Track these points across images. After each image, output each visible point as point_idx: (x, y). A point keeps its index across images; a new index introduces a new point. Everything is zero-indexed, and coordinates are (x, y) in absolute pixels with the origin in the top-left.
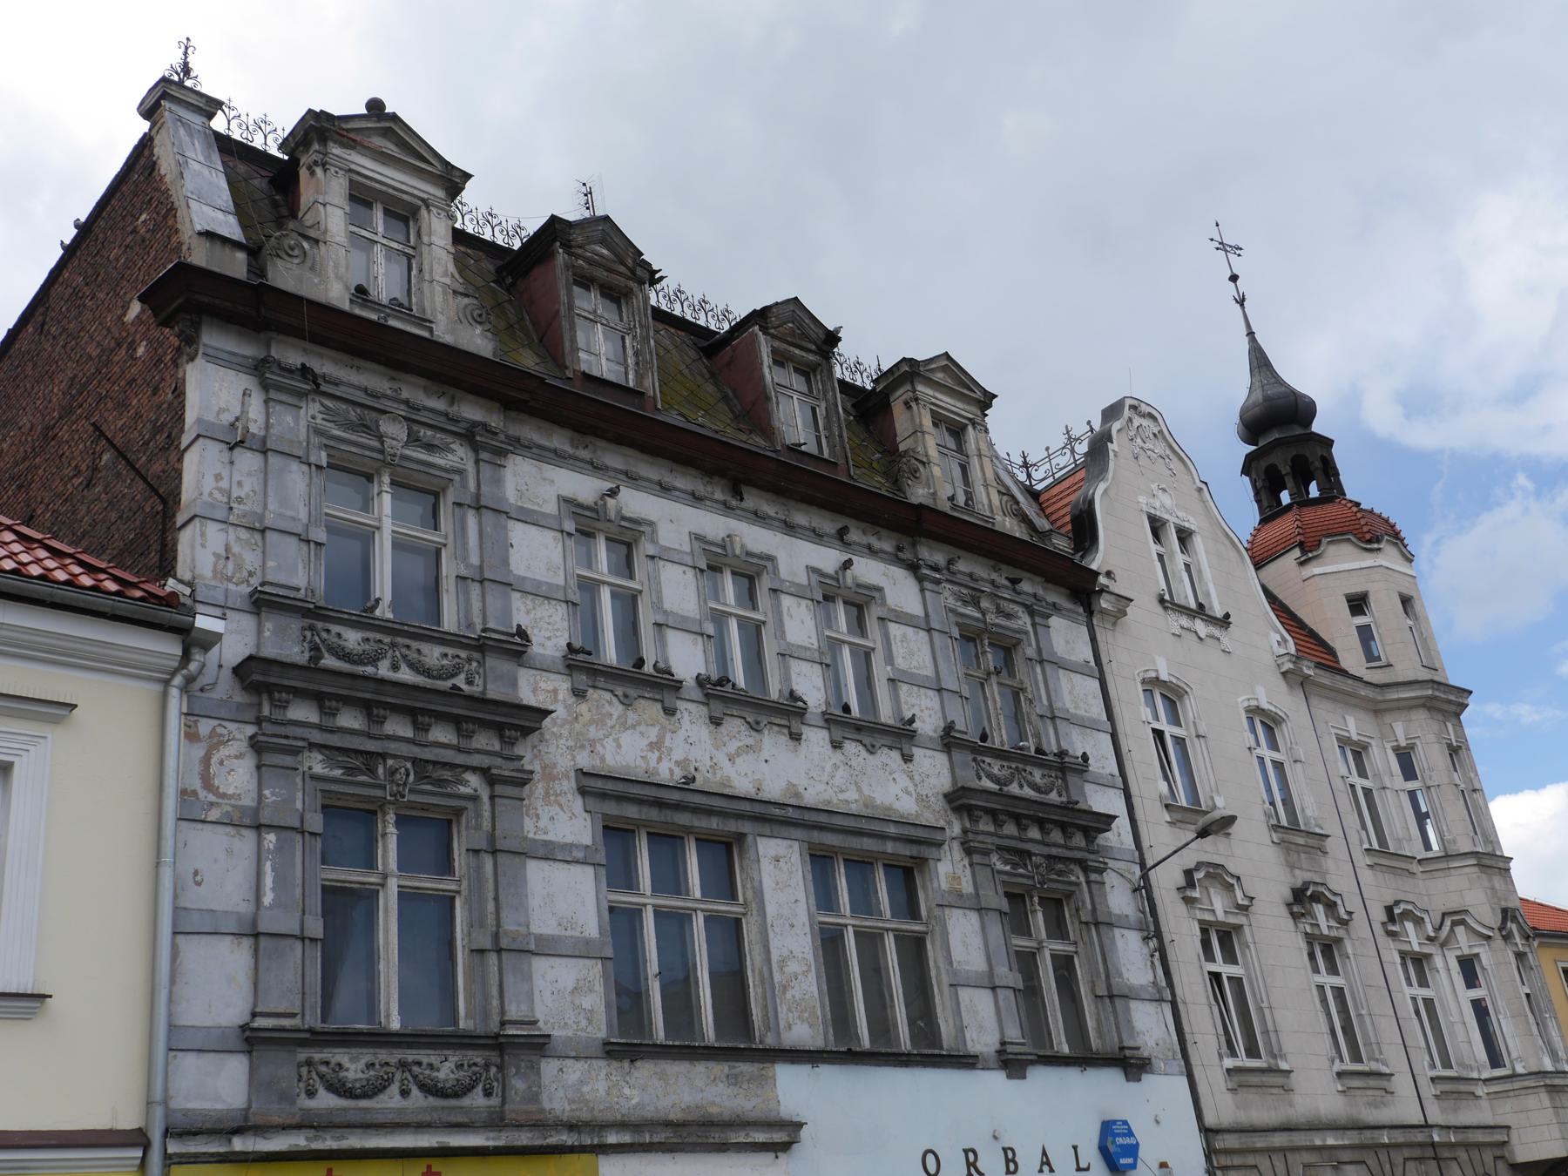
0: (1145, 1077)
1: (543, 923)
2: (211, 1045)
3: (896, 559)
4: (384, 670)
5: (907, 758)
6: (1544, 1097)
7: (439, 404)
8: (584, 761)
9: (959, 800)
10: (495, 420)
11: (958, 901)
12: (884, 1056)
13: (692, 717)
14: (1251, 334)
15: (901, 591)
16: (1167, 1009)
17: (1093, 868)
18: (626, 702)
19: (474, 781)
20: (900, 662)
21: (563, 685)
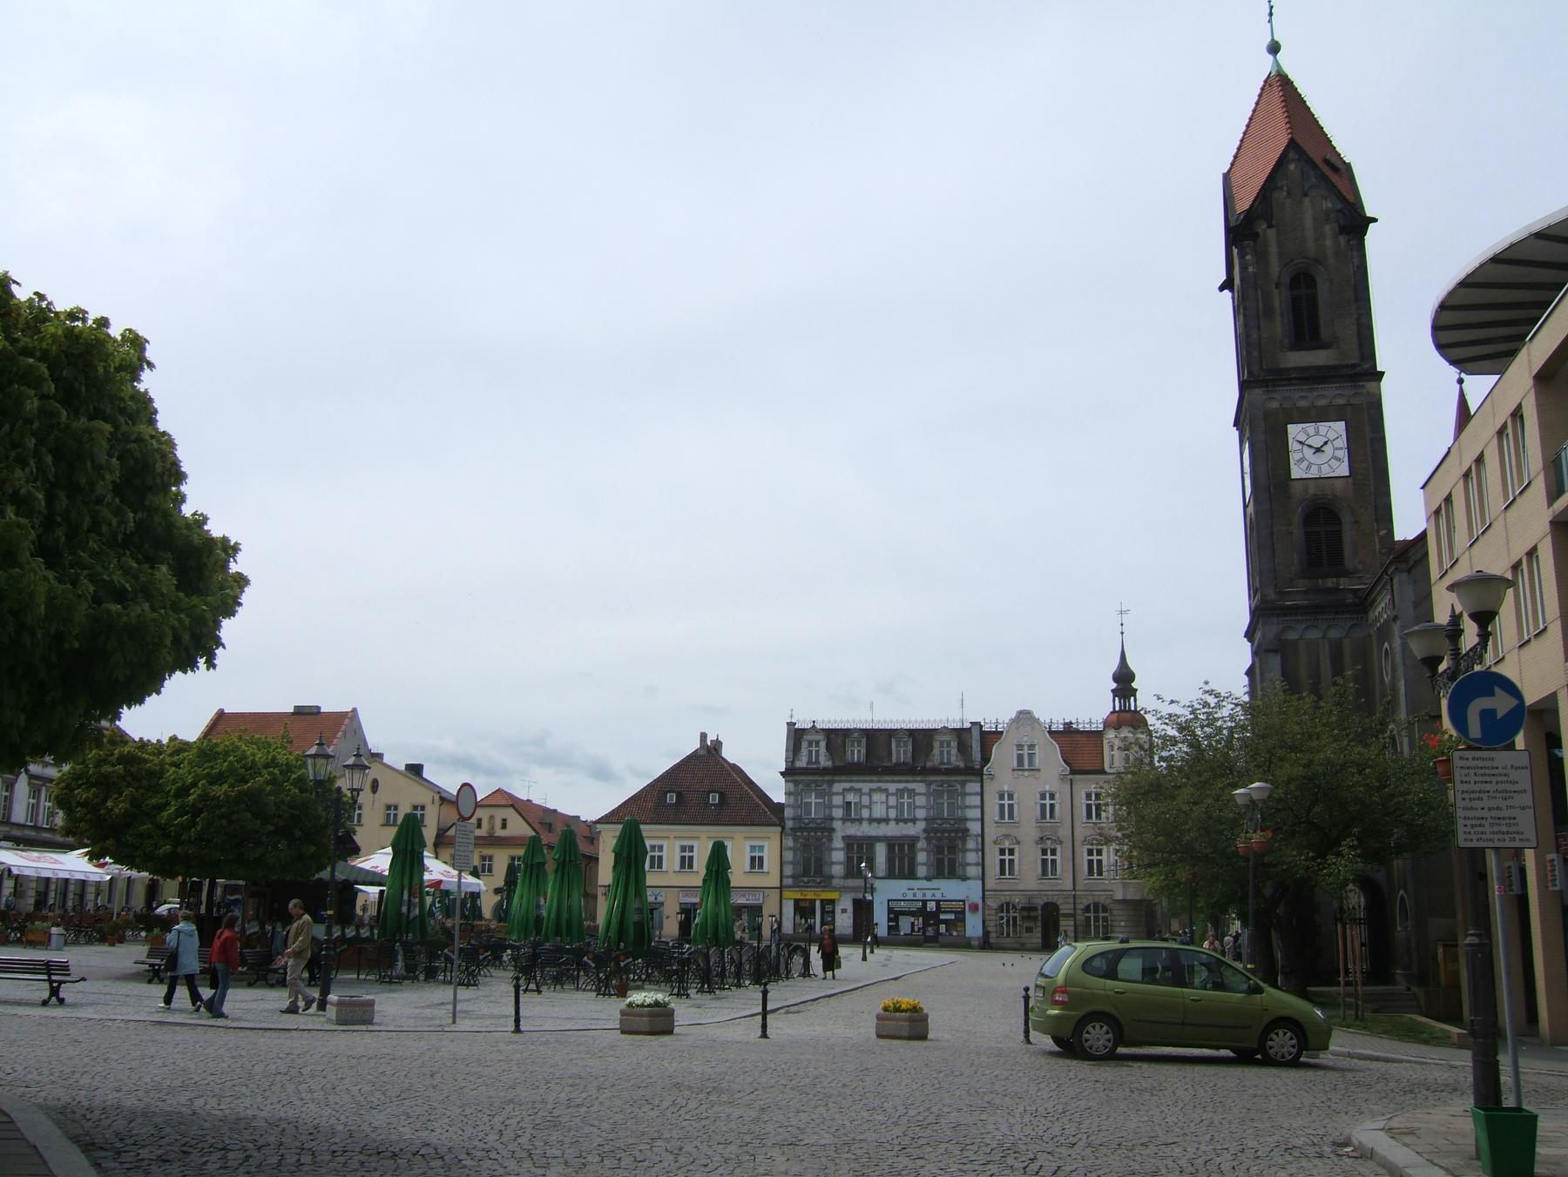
0: (968, 881)
1: (834, 860)
2: (788, 877)
3: (921, 781)
4: (811, 825)
5: (914, 823)
6: (1121, 886)
7: (820, 779)
8: (844, 834)
9: (925, 831)
10: (831, 778)
11: (922, 850)
12: (902, 876)
13: (865, 824)
14: (1123, 646)
15: (920, 787)
16: (980, 868)
17: (964, 839)
18: (852, 823)
19: (824, 840)
20: (917, 804)
21: (840, 823)
